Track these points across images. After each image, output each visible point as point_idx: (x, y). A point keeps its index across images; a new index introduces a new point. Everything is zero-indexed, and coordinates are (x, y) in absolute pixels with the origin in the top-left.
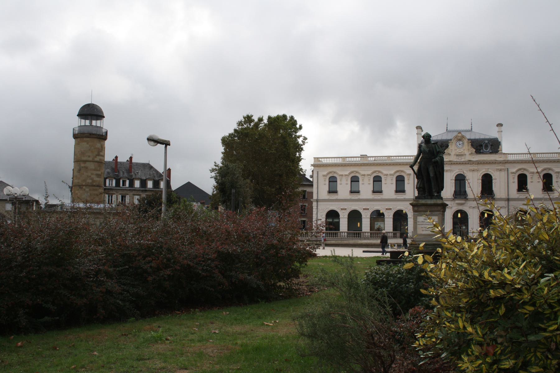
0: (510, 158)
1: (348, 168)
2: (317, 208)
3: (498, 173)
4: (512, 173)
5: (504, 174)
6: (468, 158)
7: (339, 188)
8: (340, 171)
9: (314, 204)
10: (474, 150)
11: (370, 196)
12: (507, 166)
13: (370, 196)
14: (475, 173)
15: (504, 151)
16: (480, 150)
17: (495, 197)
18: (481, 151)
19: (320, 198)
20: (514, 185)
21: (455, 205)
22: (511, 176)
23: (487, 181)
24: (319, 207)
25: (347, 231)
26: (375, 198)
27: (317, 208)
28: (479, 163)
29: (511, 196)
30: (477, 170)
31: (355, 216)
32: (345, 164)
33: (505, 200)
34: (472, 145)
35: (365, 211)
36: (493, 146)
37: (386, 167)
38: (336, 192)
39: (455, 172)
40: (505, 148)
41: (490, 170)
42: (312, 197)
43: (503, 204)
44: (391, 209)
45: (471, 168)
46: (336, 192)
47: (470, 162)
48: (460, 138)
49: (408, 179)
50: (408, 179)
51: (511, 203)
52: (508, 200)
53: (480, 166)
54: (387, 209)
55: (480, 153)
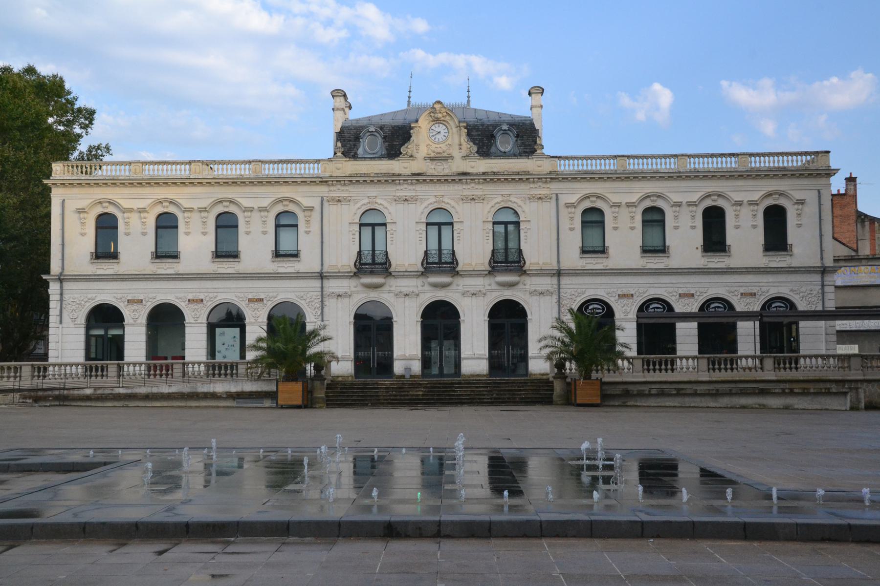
0: (564, 167)
1: (147, 190)
2: (61, 300)
3: (534, 205)
4: (568, 206)
5: (549, 207)
6: (458, 165)
7: (244, 243)
8: (246, 198)
9: (54, 289)
10: (475, 148)
11: (207, 265)
12: (555, 187)
13: (207, 265)
14: (478, 206)
15: (546, 151)
16: (489, 147)
17: (526, 267)
18: (493, 150)
19: (70, 270)
20: (573, 239)
21: (494, 286)
22: (564, 212)
23: (508, 228)
24: (66, 296)
25: (143, 359)
26: (99, 272)
27: (61, 300)
28: (355, 180)
29: (566, 265)
30: (348, 200)
31: (165, 320)
32: (202, 176)
33: (553, 275)
34: (469, 134)
35: (192, 306)
36: (526, 136)
37: (248, 189)
38: (114, 256)
39: (492, 203)
40: (551, 142)
41: (513, 199)
42: (48, 272)
43: (547, 283)
44: (261, 300)
45: (533, 192)
46: (114, 256)
47: (463, 176)
48: (438, 113)
49: (308, 222)
50: (308, 222)
51: (565, 280)
52: (322, 276)
53: (421, 190)
54: (250, 300)
55: (355, 157)
